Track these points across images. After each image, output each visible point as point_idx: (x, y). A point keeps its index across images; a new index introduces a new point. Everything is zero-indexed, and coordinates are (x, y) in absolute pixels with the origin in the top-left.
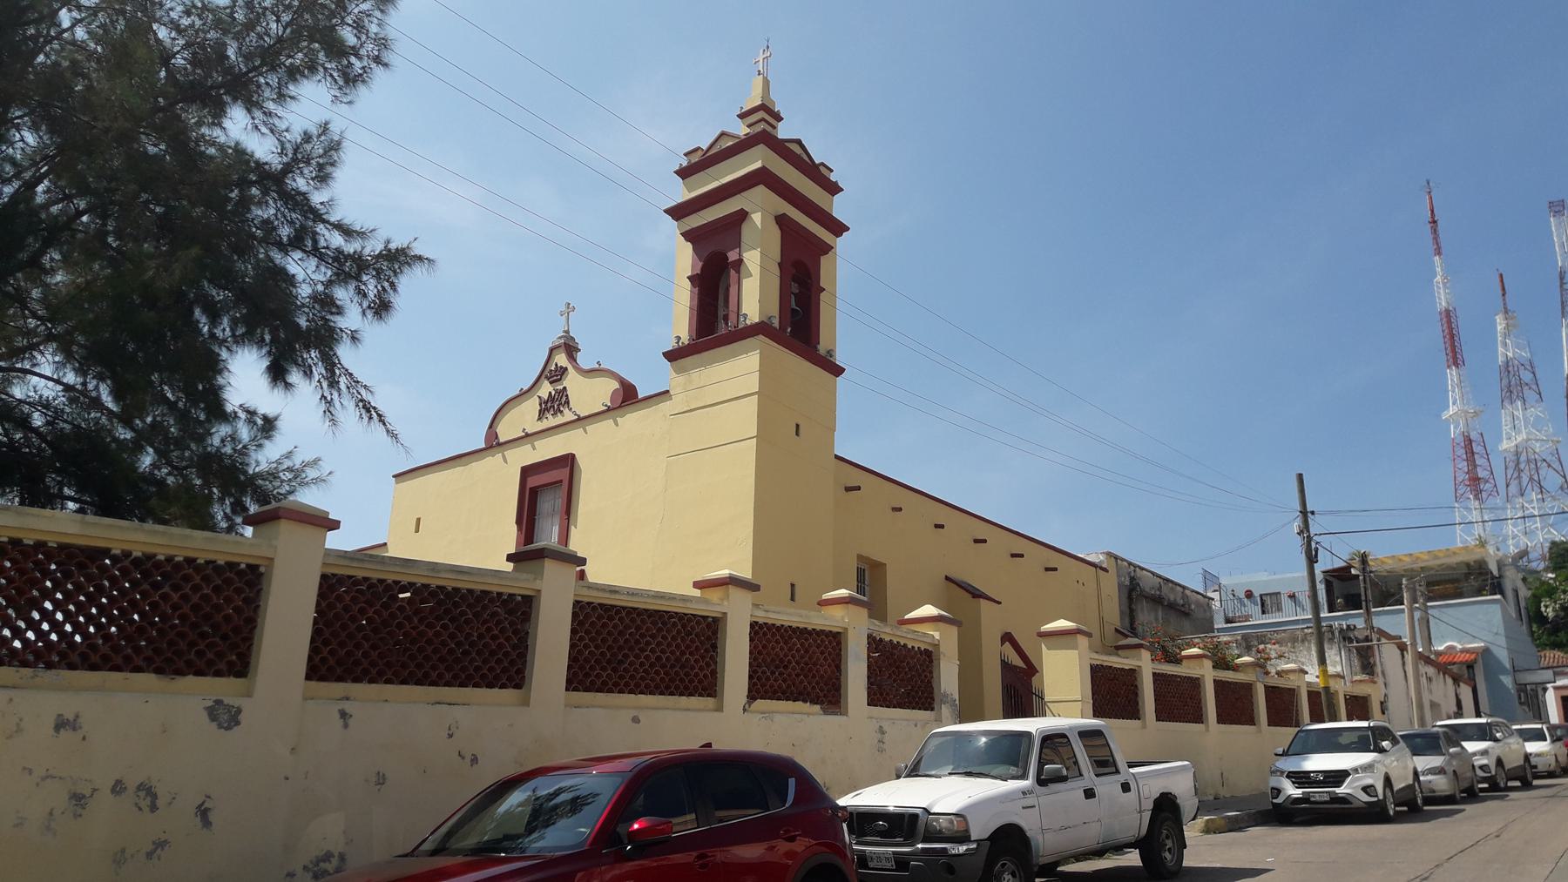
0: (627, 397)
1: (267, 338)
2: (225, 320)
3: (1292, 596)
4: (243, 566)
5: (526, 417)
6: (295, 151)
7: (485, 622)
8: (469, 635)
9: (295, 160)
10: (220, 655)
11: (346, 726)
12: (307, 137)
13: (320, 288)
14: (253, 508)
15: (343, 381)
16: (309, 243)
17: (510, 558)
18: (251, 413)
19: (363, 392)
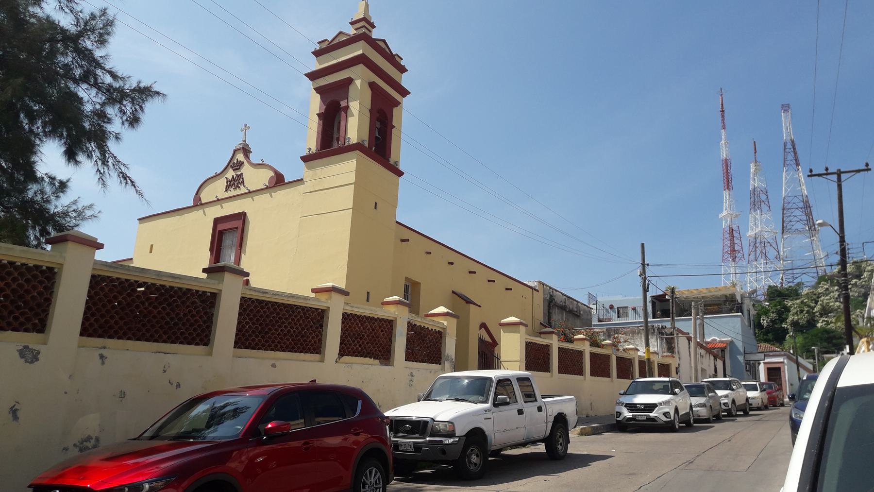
0: (278, 181)
1: (65, 134)
2: (39, 123)
3: (634, 309)
4: (44, 268)
5: (218, 189)
6: (86, 23)
7: (188, 307)
8: (178, 314)
9: (85, 30)
10: (28, 320)
11: (103, 363)
12: (93, 17)
13: (98, 107)
14: (53, 234)
15: (111, 161)
16: (92, 80)
17: (204, 270)
18: (52, 179)
19: (122, 168)
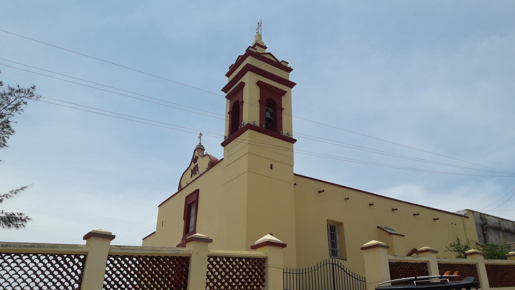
0: (213, 163)
5: (188, 178)
